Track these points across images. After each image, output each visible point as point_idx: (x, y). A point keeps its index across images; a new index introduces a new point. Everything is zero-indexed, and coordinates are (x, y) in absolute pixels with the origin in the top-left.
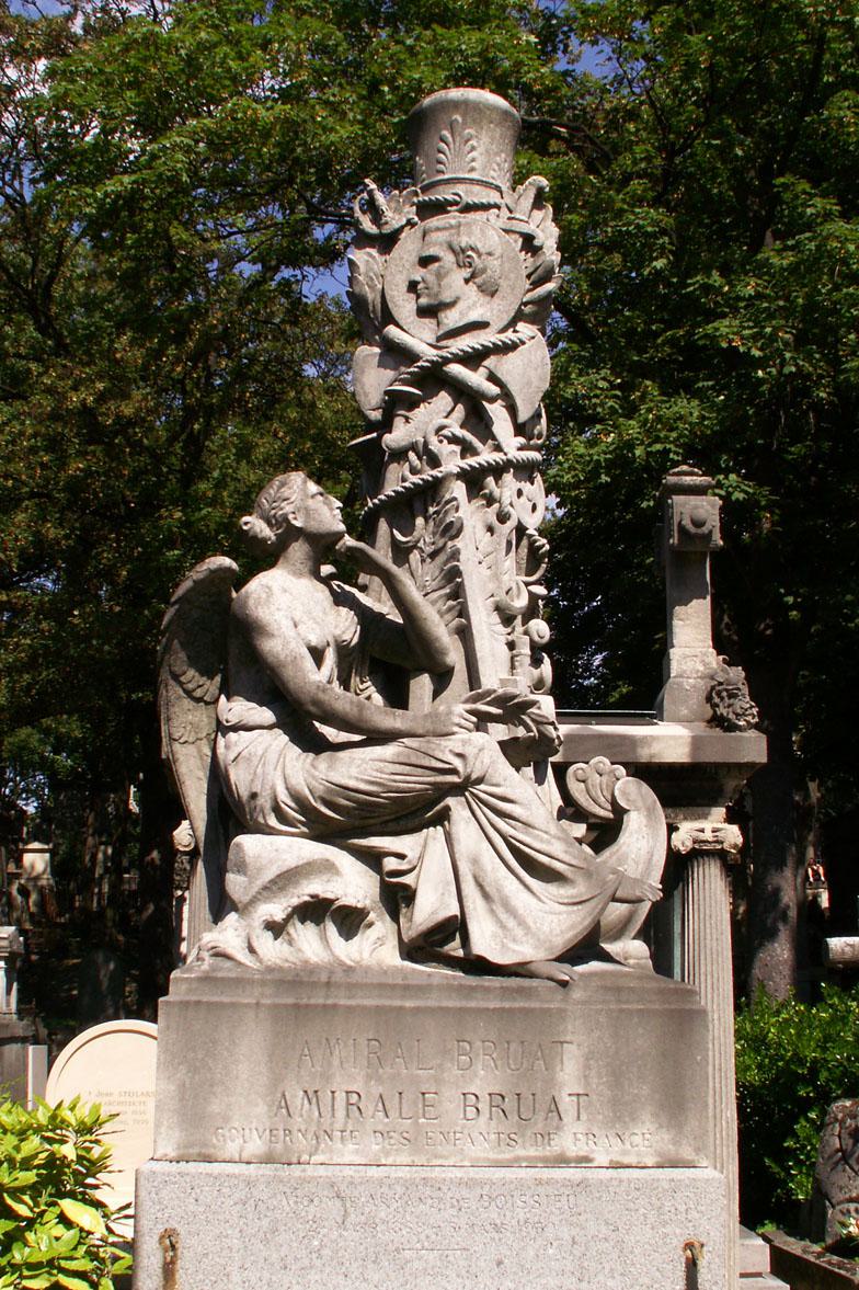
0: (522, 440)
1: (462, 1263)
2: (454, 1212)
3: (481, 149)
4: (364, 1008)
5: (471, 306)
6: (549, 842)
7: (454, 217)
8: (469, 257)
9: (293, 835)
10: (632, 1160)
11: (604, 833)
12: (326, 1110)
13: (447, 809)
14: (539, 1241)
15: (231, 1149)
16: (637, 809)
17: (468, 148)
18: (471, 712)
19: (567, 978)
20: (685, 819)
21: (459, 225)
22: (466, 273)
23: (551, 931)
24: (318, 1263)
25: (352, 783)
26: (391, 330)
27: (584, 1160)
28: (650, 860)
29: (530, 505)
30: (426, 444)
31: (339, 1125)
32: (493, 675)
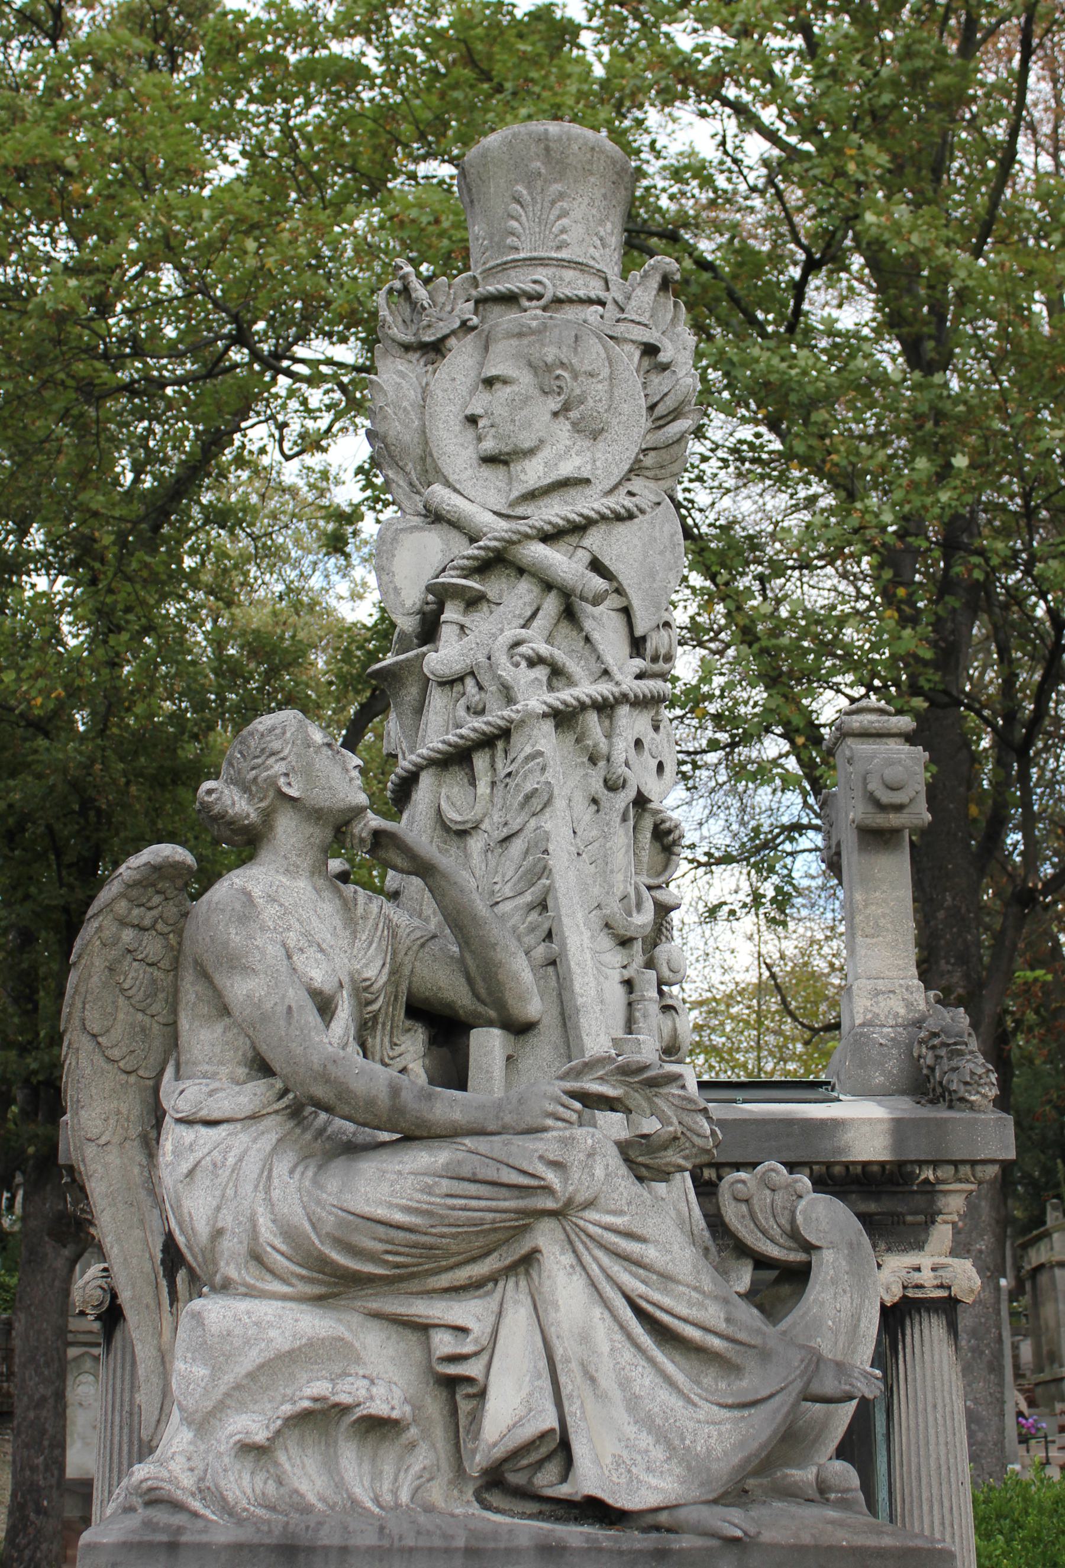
0: (638, 664)
3: (577, 213)
5: (561, 455)
6: (701, 1306)
7: (532, 315)
8: (558, 377)
9: (285, 1298)
11: (782, 1281)
13: (536, 1251)
16: (832, 1246)
17: (555, 212)
18: (573, 1095)
19: (739, 1533)
20: (889, 1250)
21: (544, 328)
23: (709, 1452)
25: (381, 1212)
26: (439, 493)
28: (856, 1327)
29: (654, 764)
32: (598, 1035)
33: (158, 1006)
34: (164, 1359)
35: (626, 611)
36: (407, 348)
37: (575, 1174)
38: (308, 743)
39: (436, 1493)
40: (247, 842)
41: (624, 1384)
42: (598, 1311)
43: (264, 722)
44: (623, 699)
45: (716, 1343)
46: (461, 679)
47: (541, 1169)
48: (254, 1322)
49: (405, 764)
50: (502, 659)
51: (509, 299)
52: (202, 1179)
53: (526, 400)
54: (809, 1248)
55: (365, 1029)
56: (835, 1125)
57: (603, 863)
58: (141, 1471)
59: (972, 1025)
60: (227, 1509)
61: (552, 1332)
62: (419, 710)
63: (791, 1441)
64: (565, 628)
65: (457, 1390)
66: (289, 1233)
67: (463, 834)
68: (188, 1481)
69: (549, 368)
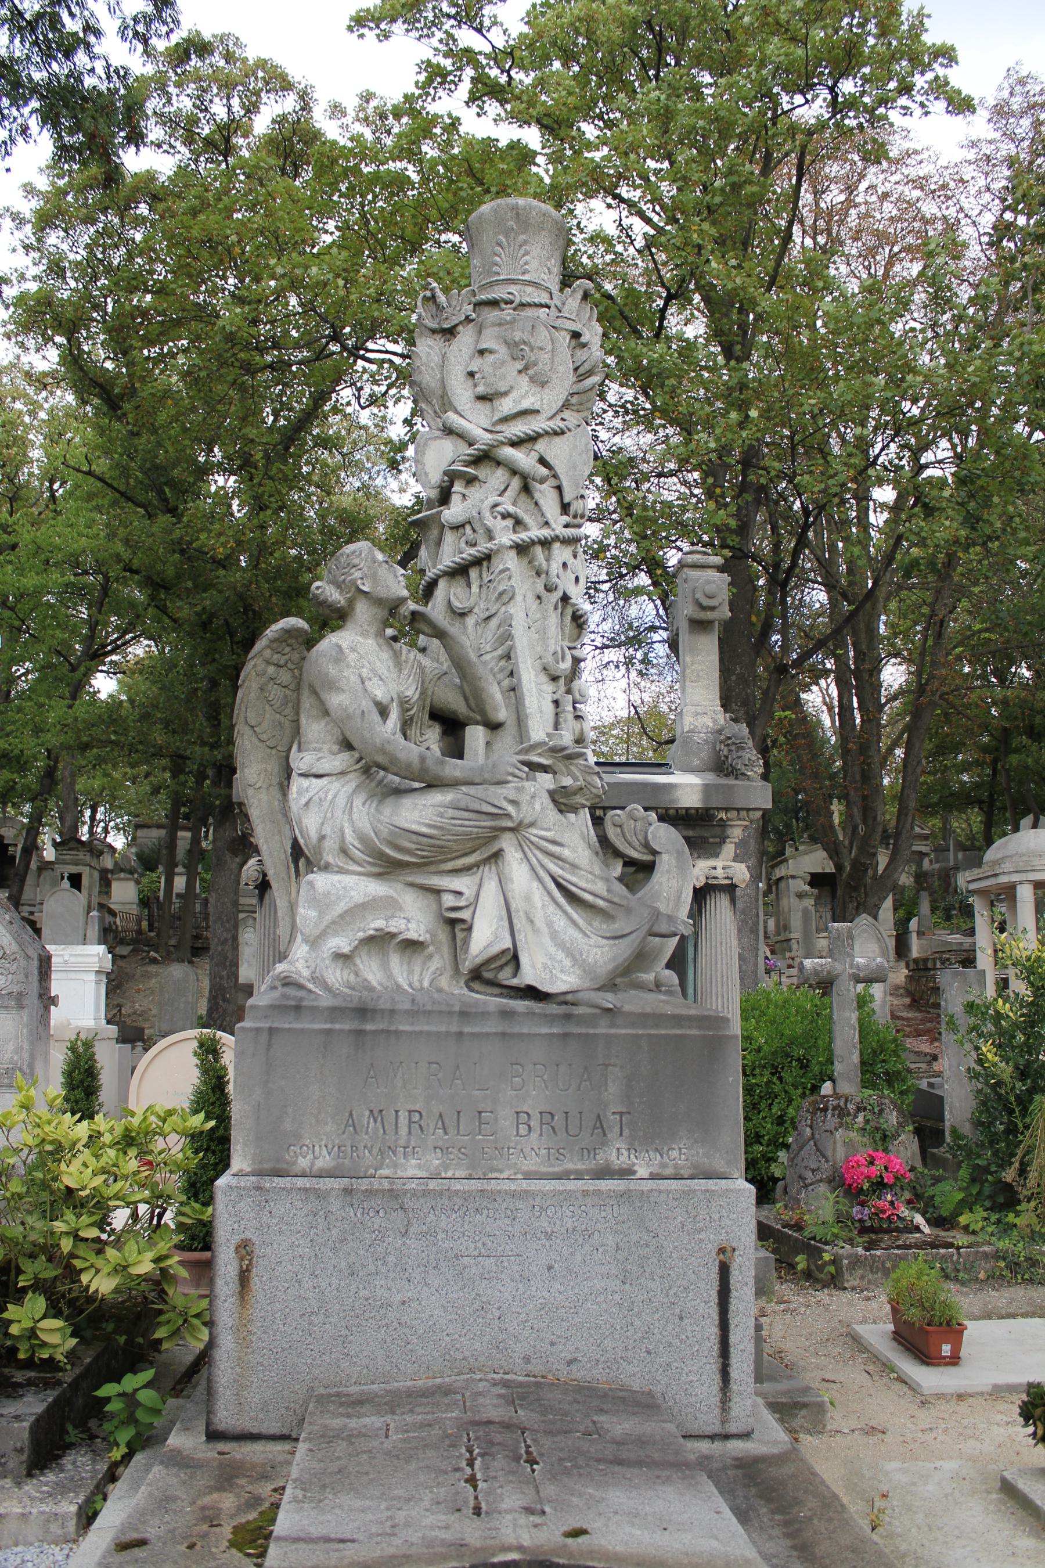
0: (565, 519)
1: (516, 1268)
2: (507, 1221)
3: (534, 253)
4: (429, 1034)
5: (523, 395)
6: (594, 882)
7: (507, 313)
9: (360, 874)
10: (669, 1171)
13: (501, 850)
14: (587, 1247)
15: (303, 1163)
16: (668, 852)
21: (514, 321)
22: (519, 365)
24: (383, 1269)
25: (414, 827)
26: (451, 417)
27: (626, 1173)
31: (402, 1142)
32: (539, 730)
34: (292, 908)
35: (559, 488)
36: (434, 331)
37: (524, 807)
38: (374, 561)
39: (444, 982)
41: (550, 924)
42: (535, 884)
43: (349, 548)
44: (556, 539)
45: (601, 903)
46: (463, 526)
47: (505, 804)
49: (430, 574)
50: (487, 514)
51: (494, 303)
52: (314, 809)
53: (503, 363)
54: (654, 853)
55: (406, 725)
56: (671, 787)
57: (543, 633)
58: (280, 968)
60: (327, 988)
61: (509, 895)
62: (439, 543)
63: (641, 958)
64: (523, 497)
65: (456, 926)
66: (362, 838)
67: (463, 615)
68: (306, 973)
69: (516, 344)
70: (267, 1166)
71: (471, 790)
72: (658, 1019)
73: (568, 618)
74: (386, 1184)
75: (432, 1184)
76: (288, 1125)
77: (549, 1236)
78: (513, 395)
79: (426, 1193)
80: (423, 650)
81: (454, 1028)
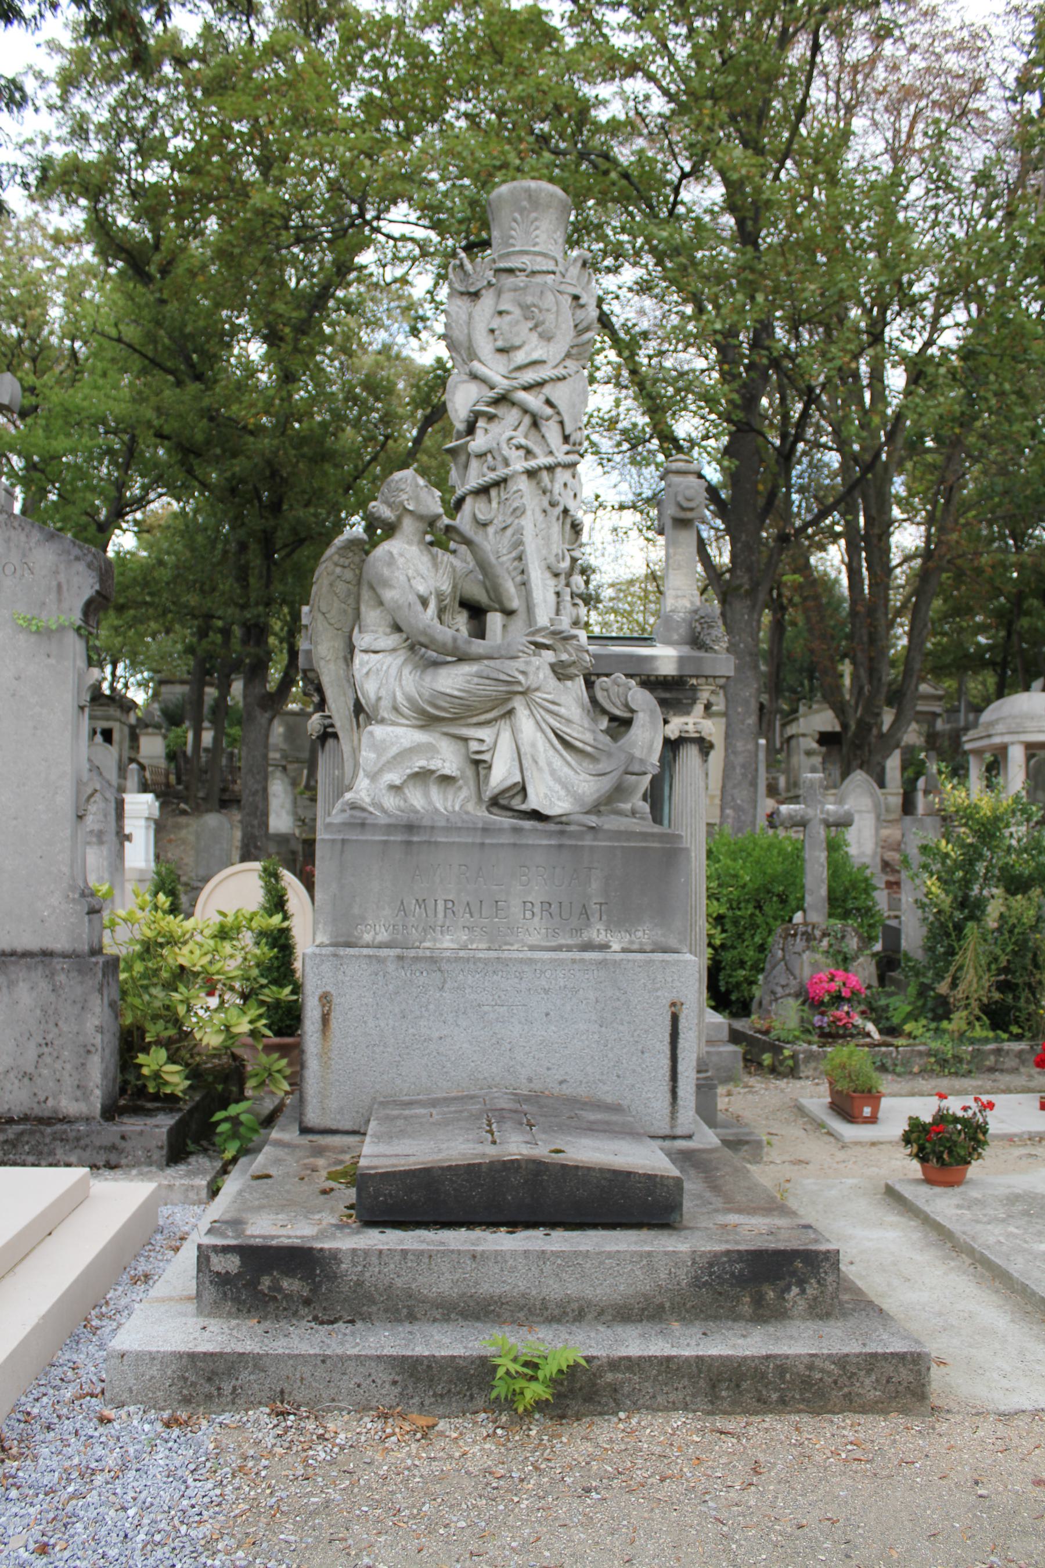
0: (566, 447)
4: (459, 844)
5: (533, 349)
7: (521, 280)
10: (635, 947)
11: (621, 724)
12: (430, 913)
15: (367, 937)
22: (530, 324)
25: (448, 691)
26: (476, 364)
27: (604, 947)
30: (499, 449)
32: (543, 617)
33: (351, 601)
34: (356, 752)
35: (562, 423)
36: (462, 294)
38: (417, 485)
39: (470, 807)
40: (391, 529)
41: (549, 764)
42: (539, 734)
43: (398, 475)
44: (558, 465)
45: (589, 749)
48: (395, 735)
49: (459, 492)
50: (504, 446)
51: (510, 271)
52: (372, 676)
53: (517, 322)
54: (632, 711)
55: (441, 611)
57: (547, 539)
58: (348, 796)
59: (723, 614)
60: (384, 811)
62: (466, 466)
63: (619, 791)
64: (533, 431)
65: (479, 765)
66: (410, 699)
67: (485, 525)
68: (367, 800)
69: (528, 307)
70: (341, 940)
71: (491, 663)
72: (630, 835)
73: (568, 526)
74: (428, 953)
75: (462, 954)
76: (356, 910)
77: (546, 991)
78: (526, 348)
79: (457, 959)
80: (454, 552)
81: (478, 840)
